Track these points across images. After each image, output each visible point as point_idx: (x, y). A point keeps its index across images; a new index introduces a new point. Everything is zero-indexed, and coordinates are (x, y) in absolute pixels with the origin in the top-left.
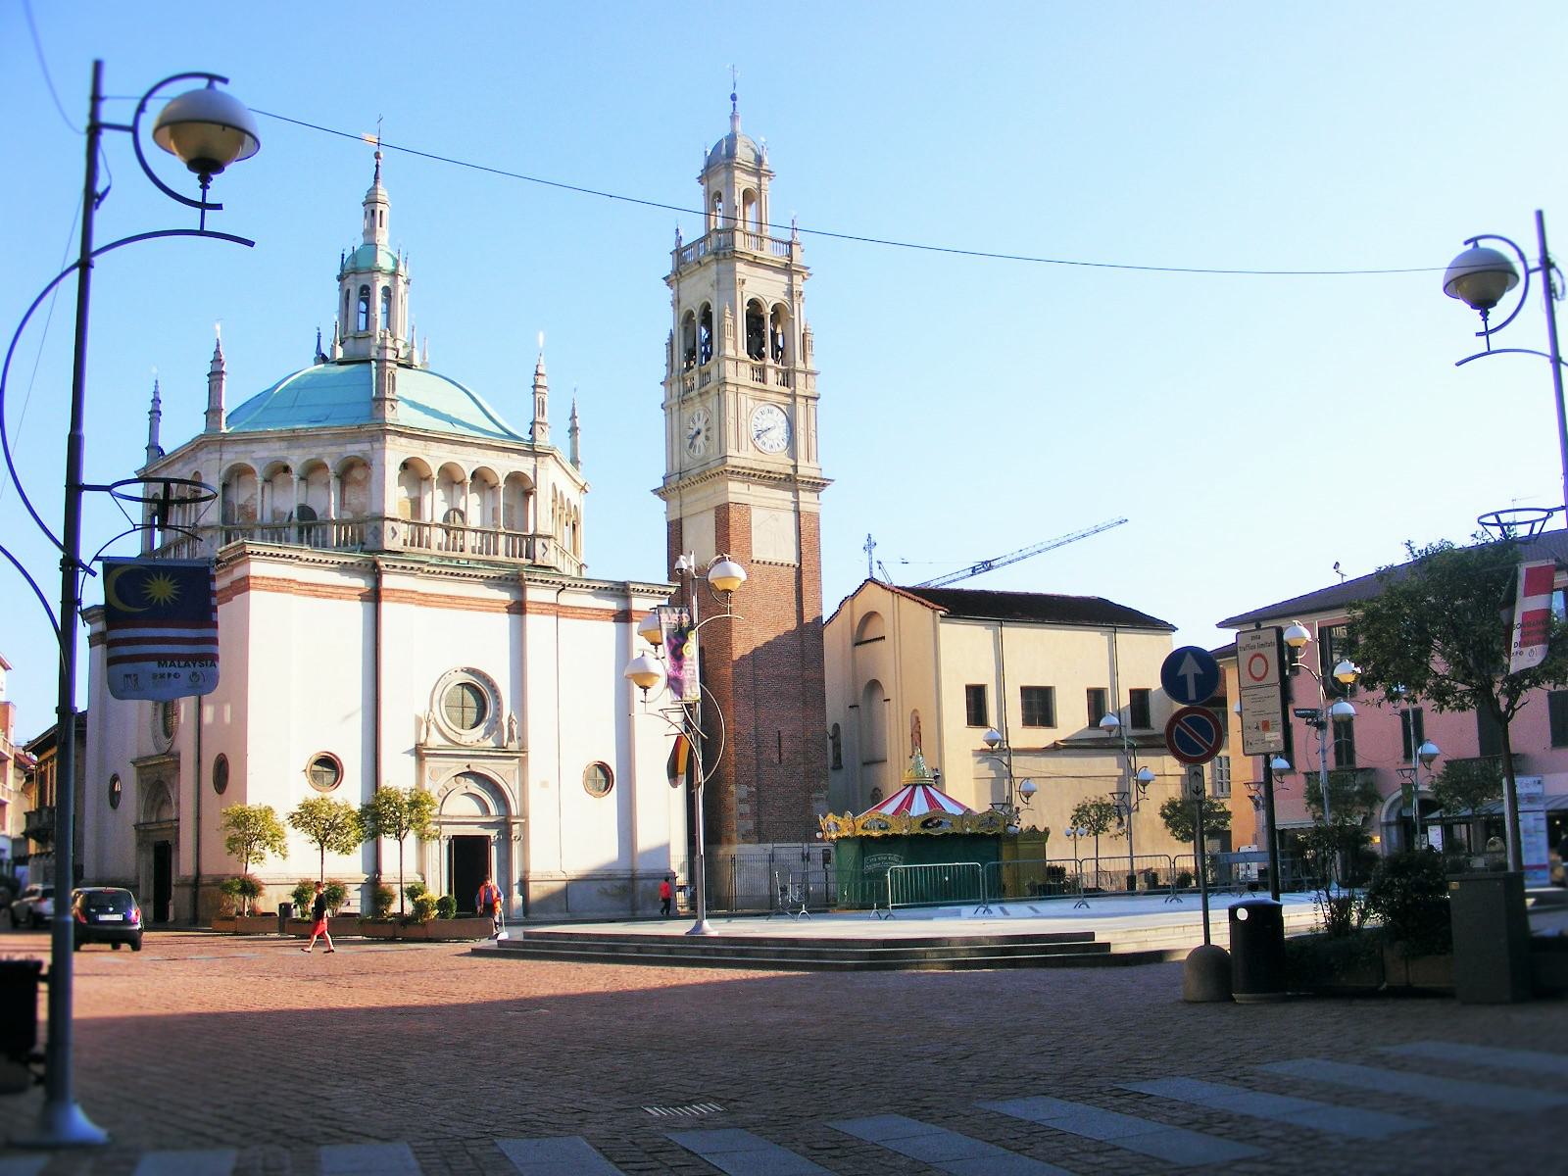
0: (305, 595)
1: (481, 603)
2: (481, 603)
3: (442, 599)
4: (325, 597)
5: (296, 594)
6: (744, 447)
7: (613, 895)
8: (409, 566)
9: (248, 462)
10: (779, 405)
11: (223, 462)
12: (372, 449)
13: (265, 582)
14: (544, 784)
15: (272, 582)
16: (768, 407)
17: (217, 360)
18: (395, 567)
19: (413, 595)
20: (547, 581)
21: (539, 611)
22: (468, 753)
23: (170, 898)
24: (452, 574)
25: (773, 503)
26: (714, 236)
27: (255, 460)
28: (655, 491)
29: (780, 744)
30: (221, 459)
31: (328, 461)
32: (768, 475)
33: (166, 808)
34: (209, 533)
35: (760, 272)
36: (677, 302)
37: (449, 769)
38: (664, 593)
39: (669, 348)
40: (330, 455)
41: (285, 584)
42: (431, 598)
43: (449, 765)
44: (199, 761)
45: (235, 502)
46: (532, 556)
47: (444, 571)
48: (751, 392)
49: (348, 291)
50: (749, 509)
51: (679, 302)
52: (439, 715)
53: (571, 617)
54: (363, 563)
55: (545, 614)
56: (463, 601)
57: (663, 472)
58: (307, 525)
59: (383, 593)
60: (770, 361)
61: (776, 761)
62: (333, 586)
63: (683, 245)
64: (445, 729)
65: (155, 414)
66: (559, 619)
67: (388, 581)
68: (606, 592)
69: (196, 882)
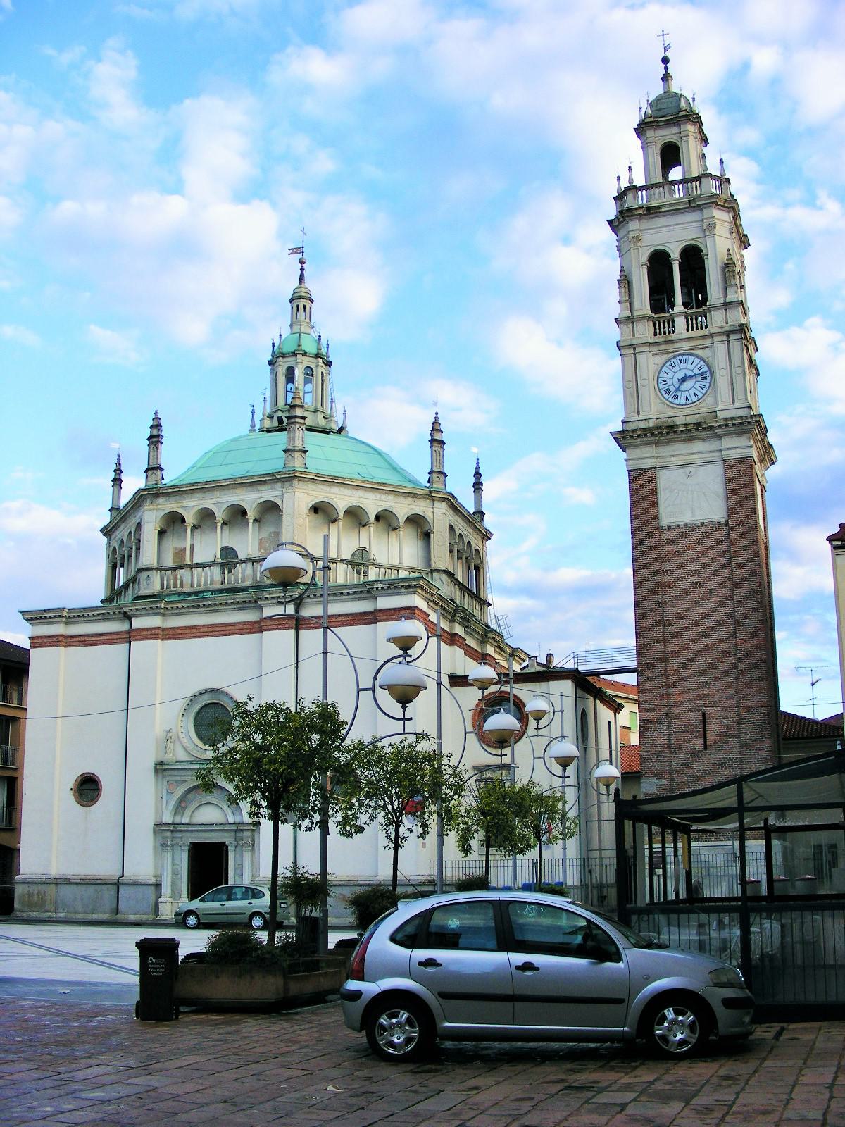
0: (76, 646)
1: (223, 628)
2: (223, 628)
3: (188, 631)
4: (91, 645)
5: (64, 646)
10: (695, 352)
15: (45, 640)
16: (680, 358)
18: (137, 609)
25: (686, 460)
35: (662, 221)
41: (55, 639)
47: (185, 605)
54: (117, 611)
60: (679, 307)
61: (699, 744)
62: (96, 635)
64: (192, 747)
67: (138, 623)
68: (349, 597)
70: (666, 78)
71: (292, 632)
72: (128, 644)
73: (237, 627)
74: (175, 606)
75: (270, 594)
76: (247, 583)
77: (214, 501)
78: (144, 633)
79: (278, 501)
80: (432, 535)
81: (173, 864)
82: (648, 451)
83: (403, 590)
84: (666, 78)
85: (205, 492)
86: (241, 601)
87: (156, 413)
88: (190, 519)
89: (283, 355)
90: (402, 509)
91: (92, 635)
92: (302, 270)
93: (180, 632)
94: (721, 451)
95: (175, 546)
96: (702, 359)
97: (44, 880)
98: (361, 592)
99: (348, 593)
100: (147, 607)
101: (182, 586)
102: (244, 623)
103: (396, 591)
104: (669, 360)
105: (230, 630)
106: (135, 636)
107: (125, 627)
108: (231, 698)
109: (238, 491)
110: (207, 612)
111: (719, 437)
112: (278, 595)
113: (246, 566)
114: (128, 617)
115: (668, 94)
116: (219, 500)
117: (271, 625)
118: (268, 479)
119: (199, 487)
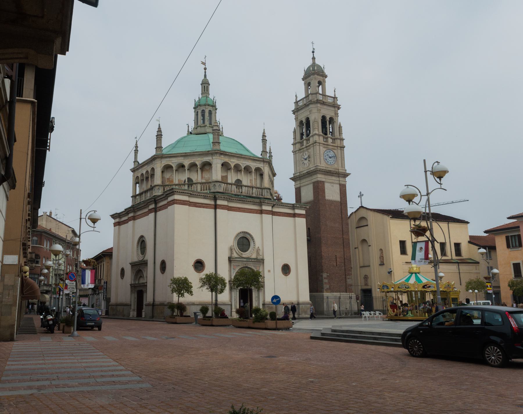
0: (192, 206)
3: (236, 209)
6: (322, 163)
9: (170, 164)
12: (213, 159)
13: (180, 202)
14: (269, 271)
15: (182, 202)
17: (159, 130)
18: (221, 197)
19: (227, 207)
20: (269, 203)
22: (245, 260)
23: (143, 309)
24: (239, 200)
26: (310, 96)
27: (173, 163)
28: (291, 179)
29: (336, 260)
31: (198, 163)
32: (330, 172)
33: (141, 279)
34: (157, 187)
35: (325, 107)
36: (296, 119)
37: (239, 265)
38: (306, 208)
39: (294, 133)
40: (198, 161)
41: (186, 202)
43: (239, 264)
44: (155, 263)
45: (166, 177)
48: (324, 146)
49: (198, 112)
50: (324, 184)
51: (297, 119)
52: (236, 246)
54: (211, 196)
55: (268, 214)
57: (293, 172)
58: (191, 184)
59: (218, 206)
61: (335, 265)
63: (298, 100)
64: (237, 252)
65: (136, 151)
67: (219, 202)
69: (153, 305)
70: (314, 58)
71: (271, 215)
73: (252, 211)
74: (233, 199)
75: (267, 201)
76: (254, 195)
77: (242, 162)
78: (222, 207)
79: (262, 168)
82: (323, 176)
83: (303, 209)
84: (314, 58)
86: (255, 202)
88: (232, 166)
89: (209, 105)
92: (205, 72)
94: (339, 181)
96: (334, 153)
99: (287, 206)
100: (226, 197)
102: (255, 210)
104: (326, 150)
106: (219, 207)
107: (212, 203)
109: (249, 161)
110: (242, 203)
111: (339, 177)
114: (215, 199)
115: (314, 64)
116: (244, 162)
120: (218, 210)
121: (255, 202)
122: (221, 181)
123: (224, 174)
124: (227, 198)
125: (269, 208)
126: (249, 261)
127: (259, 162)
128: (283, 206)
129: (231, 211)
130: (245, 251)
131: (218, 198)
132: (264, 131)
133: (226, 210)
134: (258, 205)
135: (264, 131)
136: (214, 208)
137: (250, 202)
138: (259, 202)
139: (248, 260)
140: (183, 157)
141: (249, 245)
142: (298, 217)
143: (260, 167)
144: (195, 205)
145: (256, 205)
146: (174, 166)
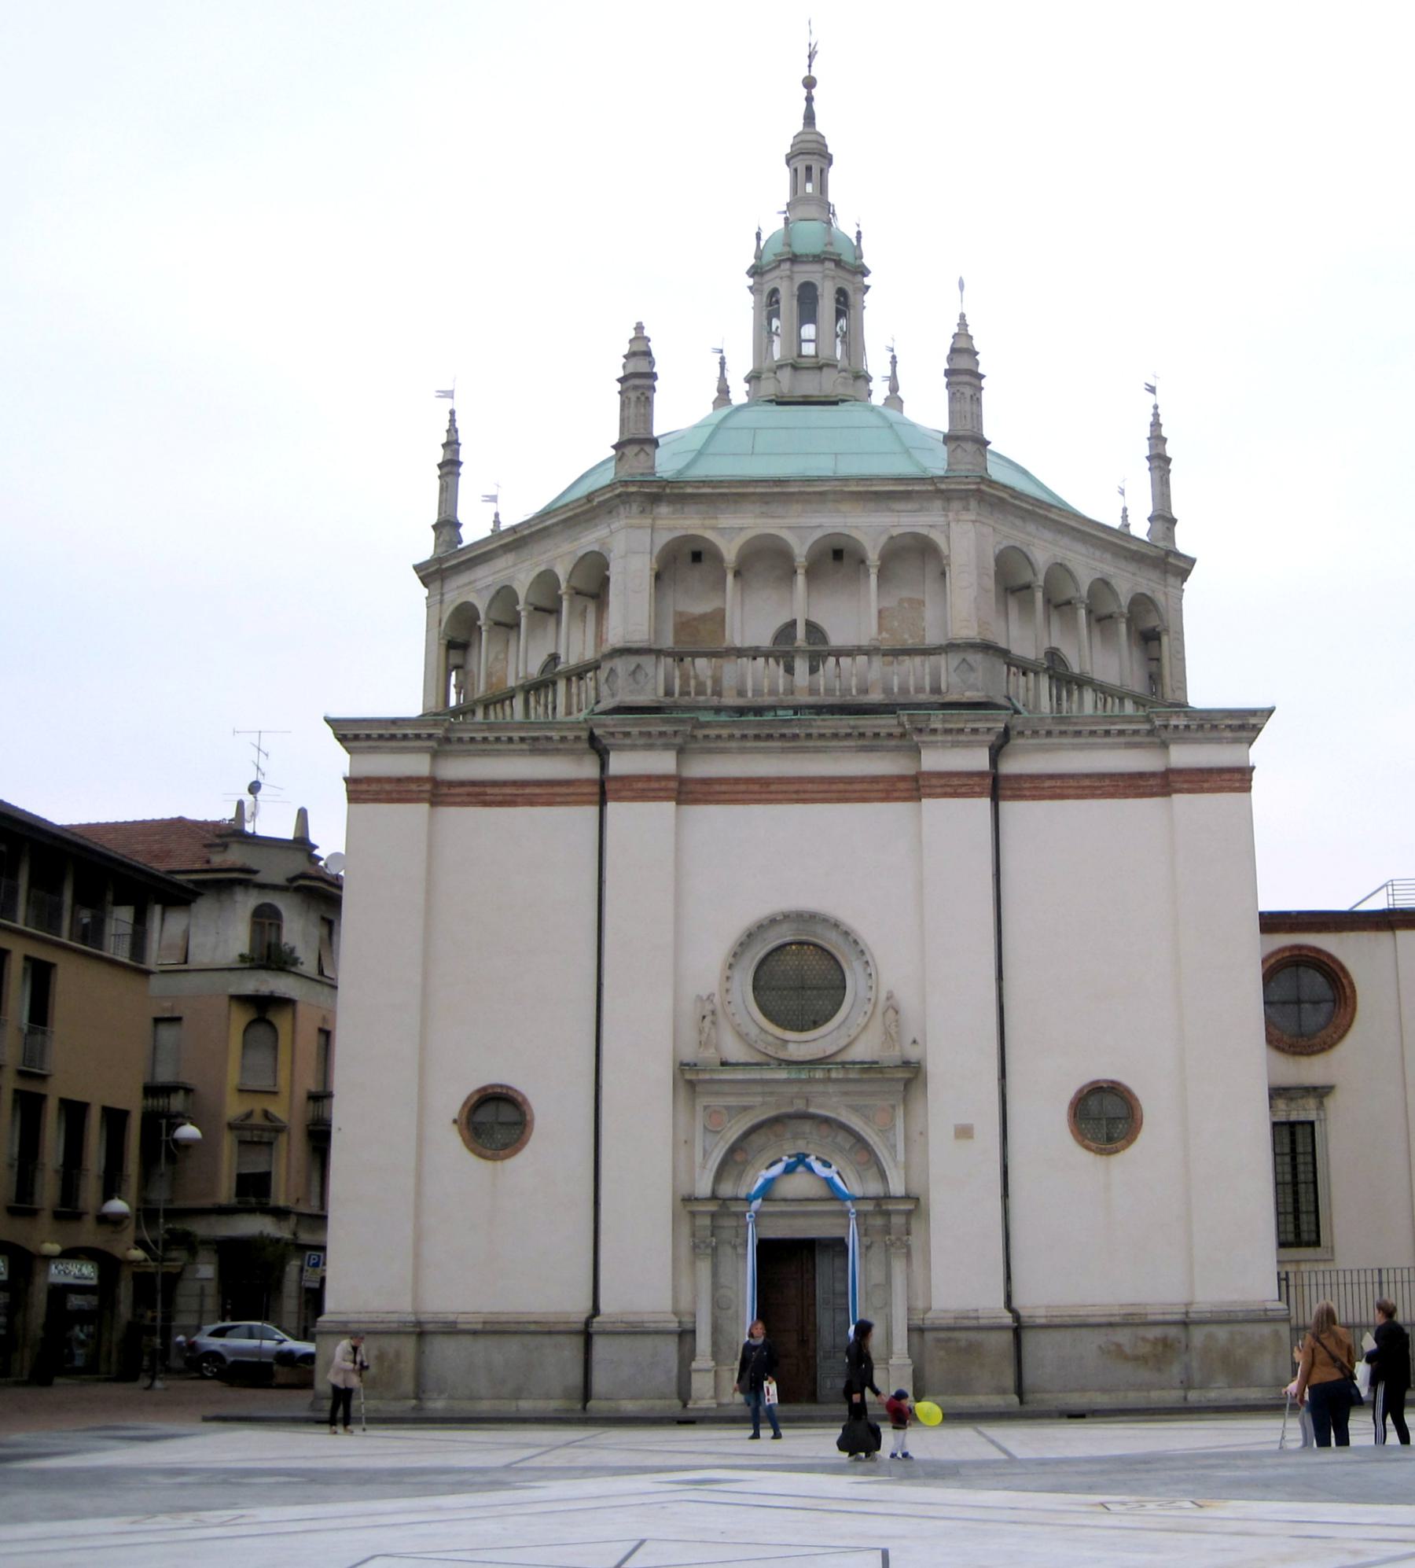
2: (825, 787)
3: (742, 787)
7: (1136, 1358)
8: (654, 729)
9: (472, 598)
11: (445, 606)
13: (374, 787)
15: (388, 787)
17: (452, 444)
18: (627, 734)
20: (961, 731)
21: (949, 790)
24: (757, 737)
27: (478, 591)
30: (441, 602)
31: (562, 571)
37: (745, 1109)
42: (717, 788)
46: (943, 687)
47: (737, 733)
53: (1034, 798)
54: (570, 735)
56: (784, 787)
59: (609, 786)
62: (515, 783)
64: (754, 1032)
66: (1004, 806)
67: (621, 764)
71: (986, 803)
72: (595, 809)
74: (712, 732)
75: (944, 721)
76: (876, 697)
78: (640, 785)
79: (937, 537)
80: (1165, 639)
81: (716, 1285)
83: (1228, 734)
85: (767, 503)
86: (869, 732)
87: (639, 328)
88: (730, 551)
90: (1127, 583)
91: (505, 783)
93: (724, 788)
95: (681, 608)
97: (395, 1325)
98: (1136, 732)
100: (654, 729)
101: (718, 692)
102: (875, 779)
103: (1215, 734)
105: (840, 792)
106: (617, 791)
107: (588, 769)
108: (846, 934)
109: (845, 507)
110: (783, 750)
112: (961, 726)
113: (870, 662)
114: (599, 749)
116: (805, 521)
117: (942, 786)
118: (917, 488)
119: (759, 490)
120: (612, 807)
121: (869, 732)
122: (645, 645)
123: (699, 607)
124: (662, 734)
125: (978, 760)
126: (809, 1081)
127: (910, 506)
128: (1078, 733)
129: (696, 801)
130: (816, 1024)
131: (612, 741)
132: (963, 323)
133: (667, 799)
134: (897, 749)
135: (963, 323)
136: (597, 798)
137: (835, 736)
138: (897, 731)
139: (804, 1076)
140: (513, 553)
141: (845, 988)
142: (1189, 791)
143: (924, 531)
144: (482, 794)
145: (889, 750)
146: (481, 606)
